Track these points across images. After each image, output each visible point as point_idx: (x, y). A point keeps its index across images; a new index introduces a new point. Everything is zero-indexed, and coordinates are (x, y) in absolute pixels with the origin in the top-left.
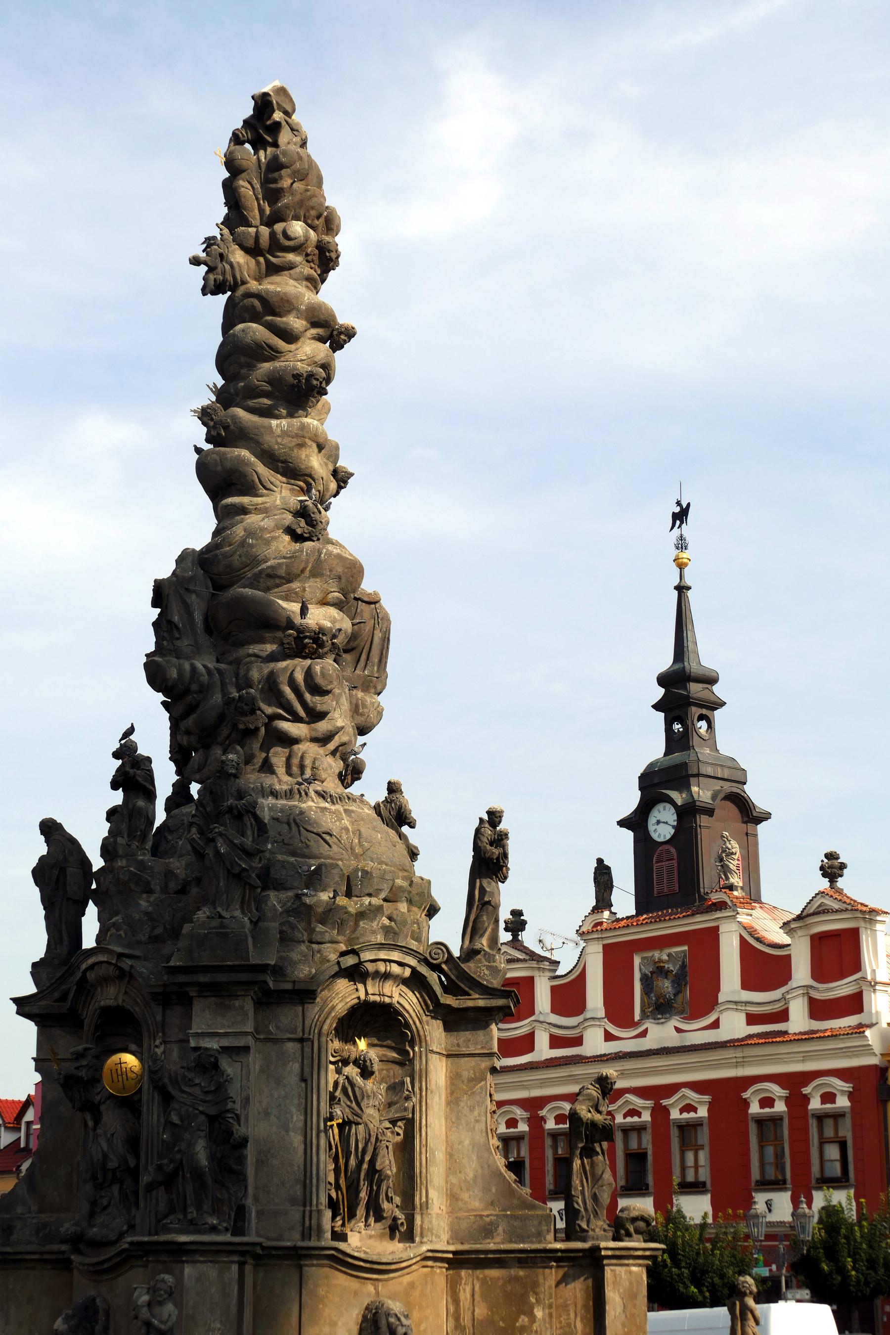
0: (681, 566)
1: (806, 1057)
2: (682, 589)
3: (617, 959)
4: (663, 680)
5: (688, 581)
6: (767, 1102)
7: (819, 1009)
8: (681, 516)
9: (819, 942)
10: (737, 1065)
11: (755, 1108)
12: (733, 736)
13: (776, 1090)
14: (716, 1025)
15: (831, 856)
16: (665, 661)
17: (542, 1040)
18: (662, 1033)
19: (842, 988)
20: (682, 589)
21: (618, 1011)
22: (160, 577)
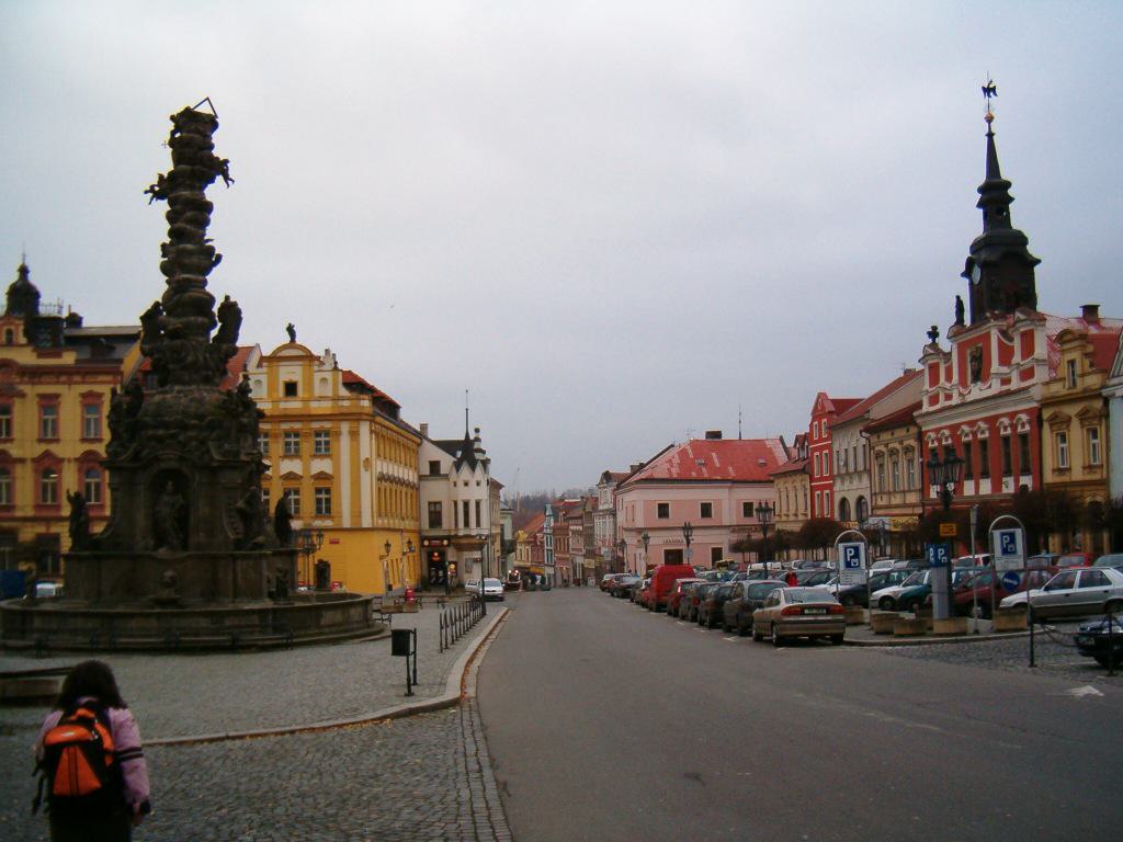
0: (990, 119)
2: (990, 135)
3: (962, 347)
4: (981, 190)
5: (993, 130)
10: (992, 409)
11: (1002, 433)
12: (1019, 218)
14: (990, 387)
16: (981, 177)
17: (942, 397)
18: (977, 391)
20: (990, 135)
21: (963, 383)
22: (142, 314)
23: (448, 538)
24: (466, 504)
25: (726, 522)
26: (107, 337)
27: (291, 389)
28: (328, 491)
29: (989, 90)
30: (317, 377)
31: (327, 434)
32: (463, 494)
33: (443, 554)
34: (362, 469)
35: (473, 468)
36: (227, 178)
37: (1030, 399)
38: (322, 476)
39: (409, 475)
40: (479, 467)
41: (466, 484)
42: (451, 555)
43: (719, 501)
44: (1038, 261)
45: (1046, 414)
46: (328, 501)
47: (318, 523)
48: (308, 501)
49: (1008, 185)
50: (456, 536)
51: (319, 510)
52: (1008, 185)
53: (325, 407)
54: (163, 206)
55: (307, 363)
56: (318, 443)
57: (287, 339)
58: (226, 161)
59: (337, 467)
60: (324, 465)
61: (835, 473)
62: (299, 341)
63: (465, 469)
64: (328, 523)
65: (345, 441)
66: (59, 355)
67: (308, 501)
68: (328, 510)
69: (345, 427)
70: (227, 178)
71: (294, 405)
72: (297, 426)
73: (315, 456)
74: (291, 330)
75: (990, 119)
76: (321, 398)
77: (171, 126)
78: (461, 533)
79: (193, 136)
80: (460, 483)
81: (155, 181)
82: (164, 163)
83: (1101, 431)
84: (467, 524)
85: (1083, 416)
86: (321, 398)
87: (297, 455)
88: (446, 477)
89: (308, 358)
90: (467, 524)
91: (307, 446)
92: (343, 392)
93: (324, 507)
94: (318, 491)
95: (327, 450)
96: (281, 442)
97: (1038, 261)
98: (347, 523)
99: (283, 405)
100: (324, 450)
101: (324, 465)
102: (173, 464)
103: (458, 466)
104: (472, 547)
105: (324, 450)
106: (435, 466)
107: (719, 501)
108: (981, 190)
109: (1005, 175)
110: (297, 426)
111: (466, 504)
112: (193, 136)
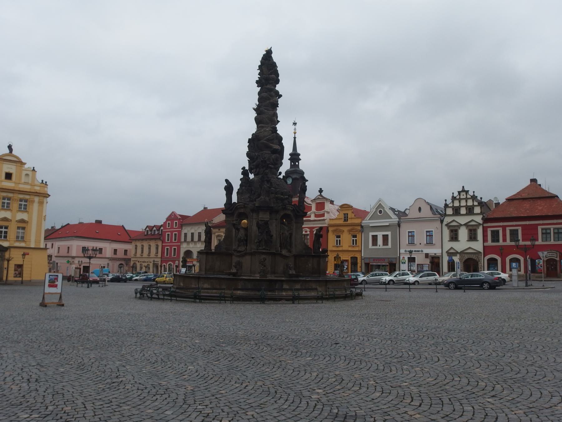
0: (295, 133)
1: (314, 224)
2: (295, 138)
4: (290, 155)
6: (306, 232)
7: (316, 216)
8: (295, 124)
9: (317, 204)
11: (304, 233)
12: (302, 165)
13: (308, 230)
15: (321, 189)
19: (321, 212)
20: (295, 138)
25: (107, 256)
27: (9, 176)
29: (295, 124)
30: (24, 173)
31: (26, 201)
37: (325, 223)
38: (22, 221)
43: (106, 248)
44: (307, 181)
45: (330, 229)
47: (17, 244)
49: (299, 155)
52: (299, 155)
55: (19, 165)
56: (21, 205)
57: (7, 151)
59: (31, 218)
60: (24, 216)
61: (183, 240)
62: (14, 152)
64: (23, 245)
65: (36, 206)
69: (36, 199)
72: (10, 195)
74: (10, 147)
75: (295, 133)
83: (359, 236)
85: (349, 231)
89: (19, 163)
91: (15, 206)
94: (18, 228)
95: (26, 209)
97: (307, 181)
98: (33, 246)
100: (24, 208)
101: (24, 216)
102: (289, 212)
105: (24, 208)
107: (106, 248)
108: (290, 155)
109: (298, 151)
110: (10, 195)
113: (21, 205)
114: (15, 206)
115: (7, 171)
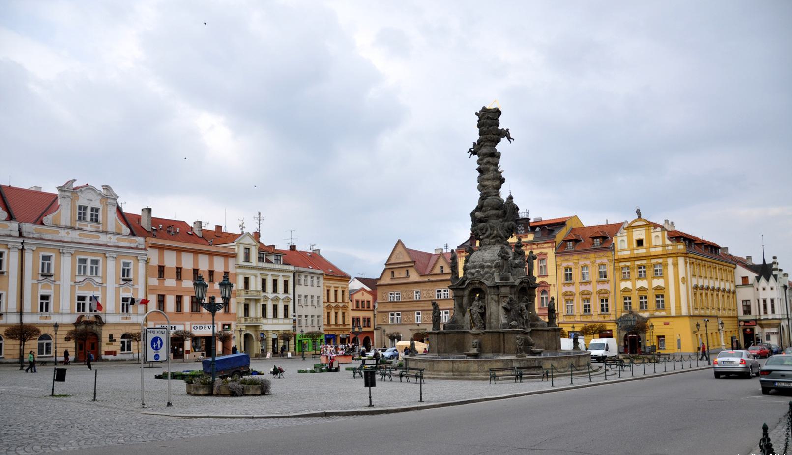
23: (756, 320)
24: (765, 301)
26: (548, 225)
27: (640, 243)
28: (662, 296)
30: (654, 235)
32: (762, 295)
33: (752, 330)
34: (681, 284)
35: (768, 280)
36: (509, 138)
38: (658, 288)
39: (728, 286)
40: (772, 279)
41: (764, 289)
42: (757, 330)
46: (663, 301)
47: (658, 314)
48: (652, 301)
50: (760, 320)
51: (658, 307)
53: (659, 250)
54: (476, 158)
57: (636, 217)
58: (508, 130)
59: (667, 283)
60: (659, 282)
63: (763, 280)
64: (663, 313)
65: (670, 268)
66: (526, 236)
67: (652, 301)
68: (663, 306)
69: (670, 261)
70: (509, 138)
71: (642, 251)
72: (644, 262)
73: (654, 278)
74: (638, 212)
76: (656, 247)
77: (477, 118)
78: (762, 318)
79: (489, 120)
80: (760, 289)
81: (472, 146)
82: (474, 135)
84: (766, 313)
86: (656, 247)
87: (645, 278)
88: (752, 285)
90: (766, 313)
91: (650, 273)
92: (668, 242)
93: (661, 303)
94: (657, 296)
96: (637, 270)
98: (673, 313)
99: (636, 252)
100: (658, 274)
101: (659, 282)
103: (758, 279)
104: (770, 326)
106: (745, 279)
111: (765, 301)
112: (489, 120)
113: (640, 272)
114: (635, 274)
115: (637, 238)
